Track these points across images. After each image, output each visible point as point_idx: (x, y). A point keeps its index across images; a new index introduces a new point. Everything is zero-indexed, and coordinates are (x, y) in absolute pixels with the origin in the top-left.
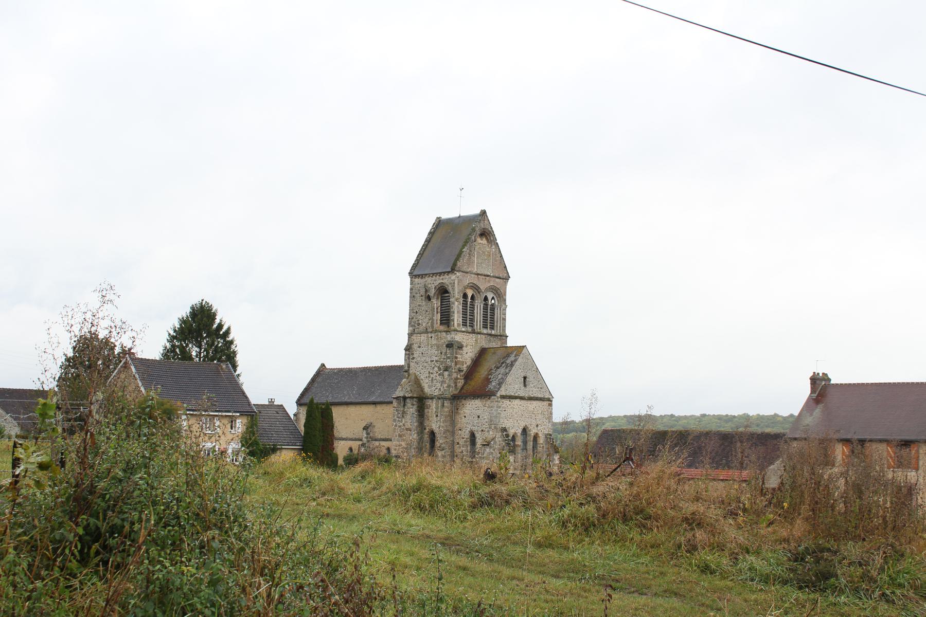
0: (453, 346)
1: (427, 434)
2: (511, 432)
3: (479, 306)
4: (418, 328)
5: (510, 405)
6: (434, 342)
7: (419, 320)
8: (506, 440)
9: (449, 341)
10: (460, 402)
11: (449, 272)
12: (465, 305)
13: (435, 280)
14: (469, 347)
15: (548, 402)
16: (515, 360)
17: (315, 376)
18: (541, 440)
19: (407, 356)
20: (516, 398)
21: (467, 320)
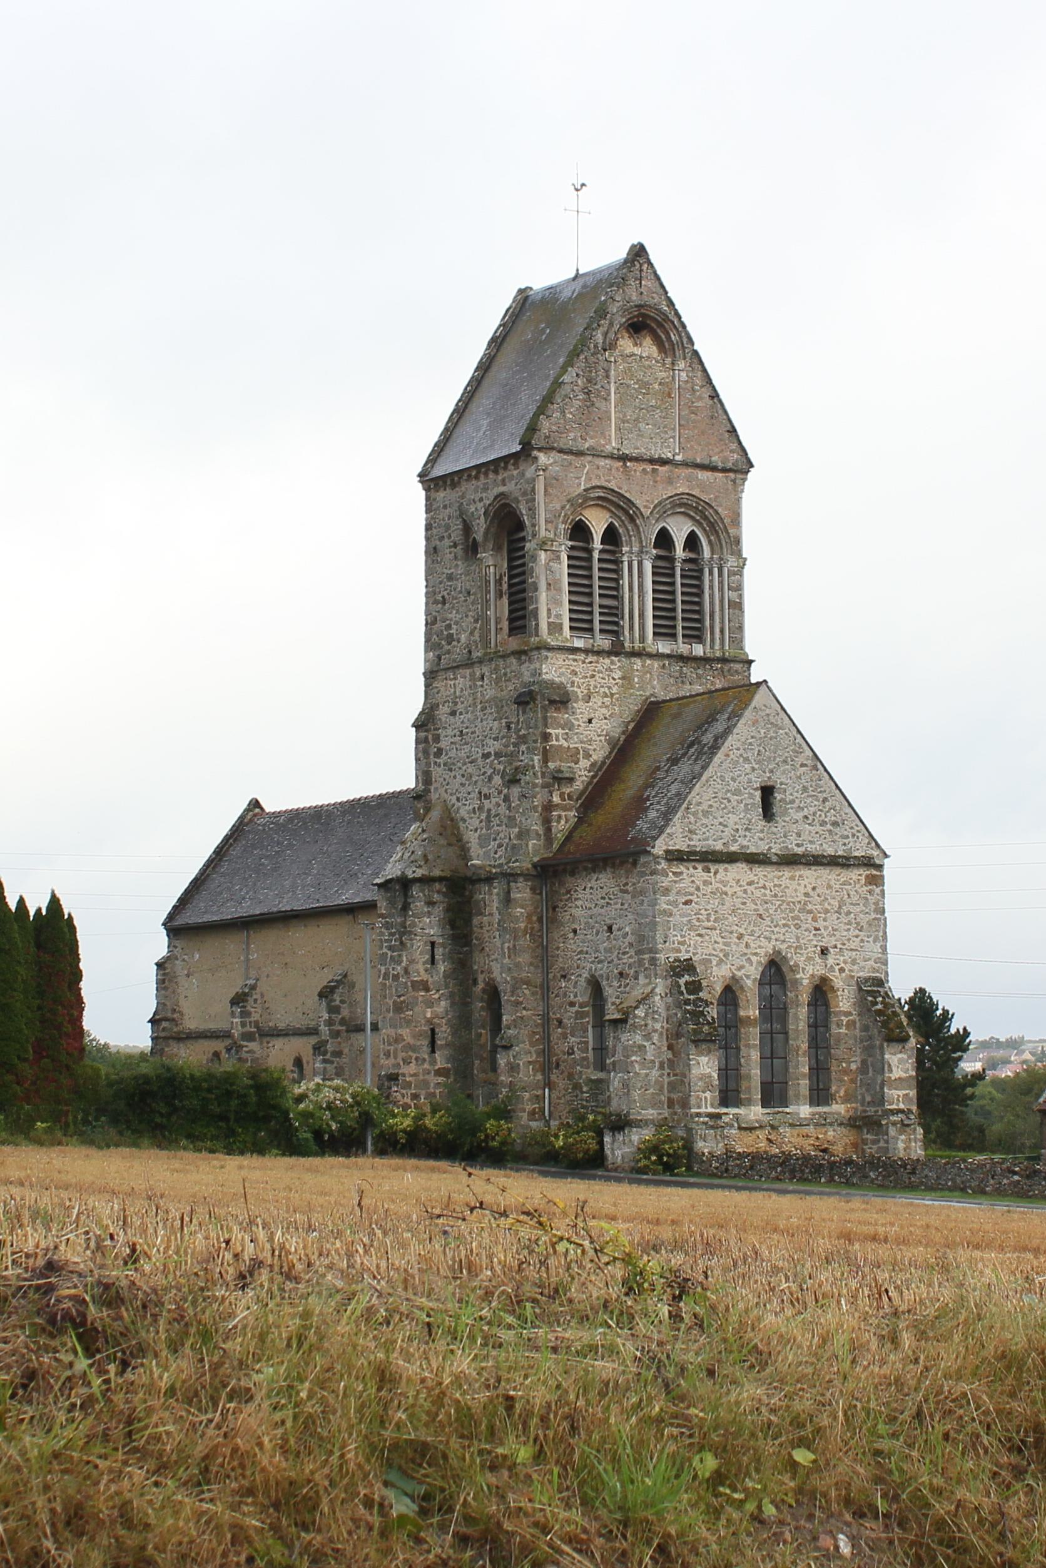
0: (534, 699)
1: (482, 1000)
2: (716, 977)
3: (635, 564)
4: (449, 652)
5: (706, 883)
6: (490, 693)
7: (449, 627)
8: (687, 1002)
9: (524, 685)
10: (562, 883)
11: (515, 456)
12: (580, 561)
13: (486, 489)
14: (597, 700)
15: (864, 872)
16: (727, 731)
17: (227, 839)
18: (844, 1001)
19: (421, 747)
20: (731, 858)
21: (591, 613)
